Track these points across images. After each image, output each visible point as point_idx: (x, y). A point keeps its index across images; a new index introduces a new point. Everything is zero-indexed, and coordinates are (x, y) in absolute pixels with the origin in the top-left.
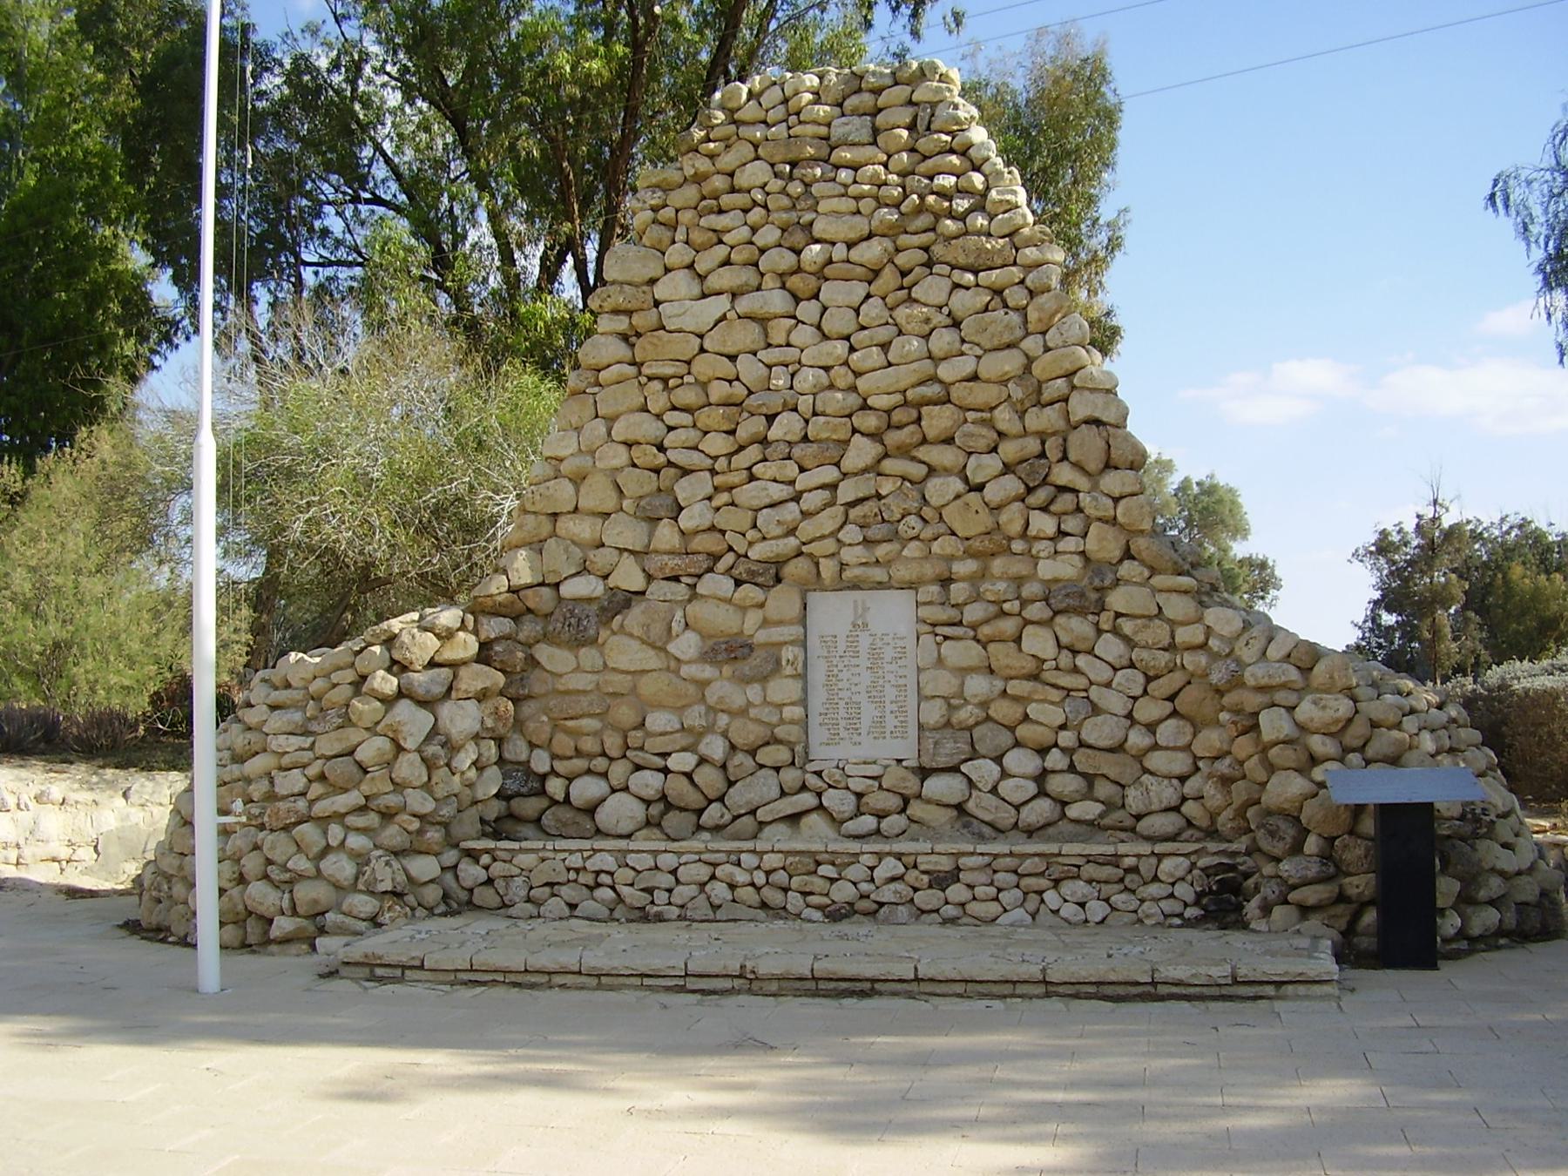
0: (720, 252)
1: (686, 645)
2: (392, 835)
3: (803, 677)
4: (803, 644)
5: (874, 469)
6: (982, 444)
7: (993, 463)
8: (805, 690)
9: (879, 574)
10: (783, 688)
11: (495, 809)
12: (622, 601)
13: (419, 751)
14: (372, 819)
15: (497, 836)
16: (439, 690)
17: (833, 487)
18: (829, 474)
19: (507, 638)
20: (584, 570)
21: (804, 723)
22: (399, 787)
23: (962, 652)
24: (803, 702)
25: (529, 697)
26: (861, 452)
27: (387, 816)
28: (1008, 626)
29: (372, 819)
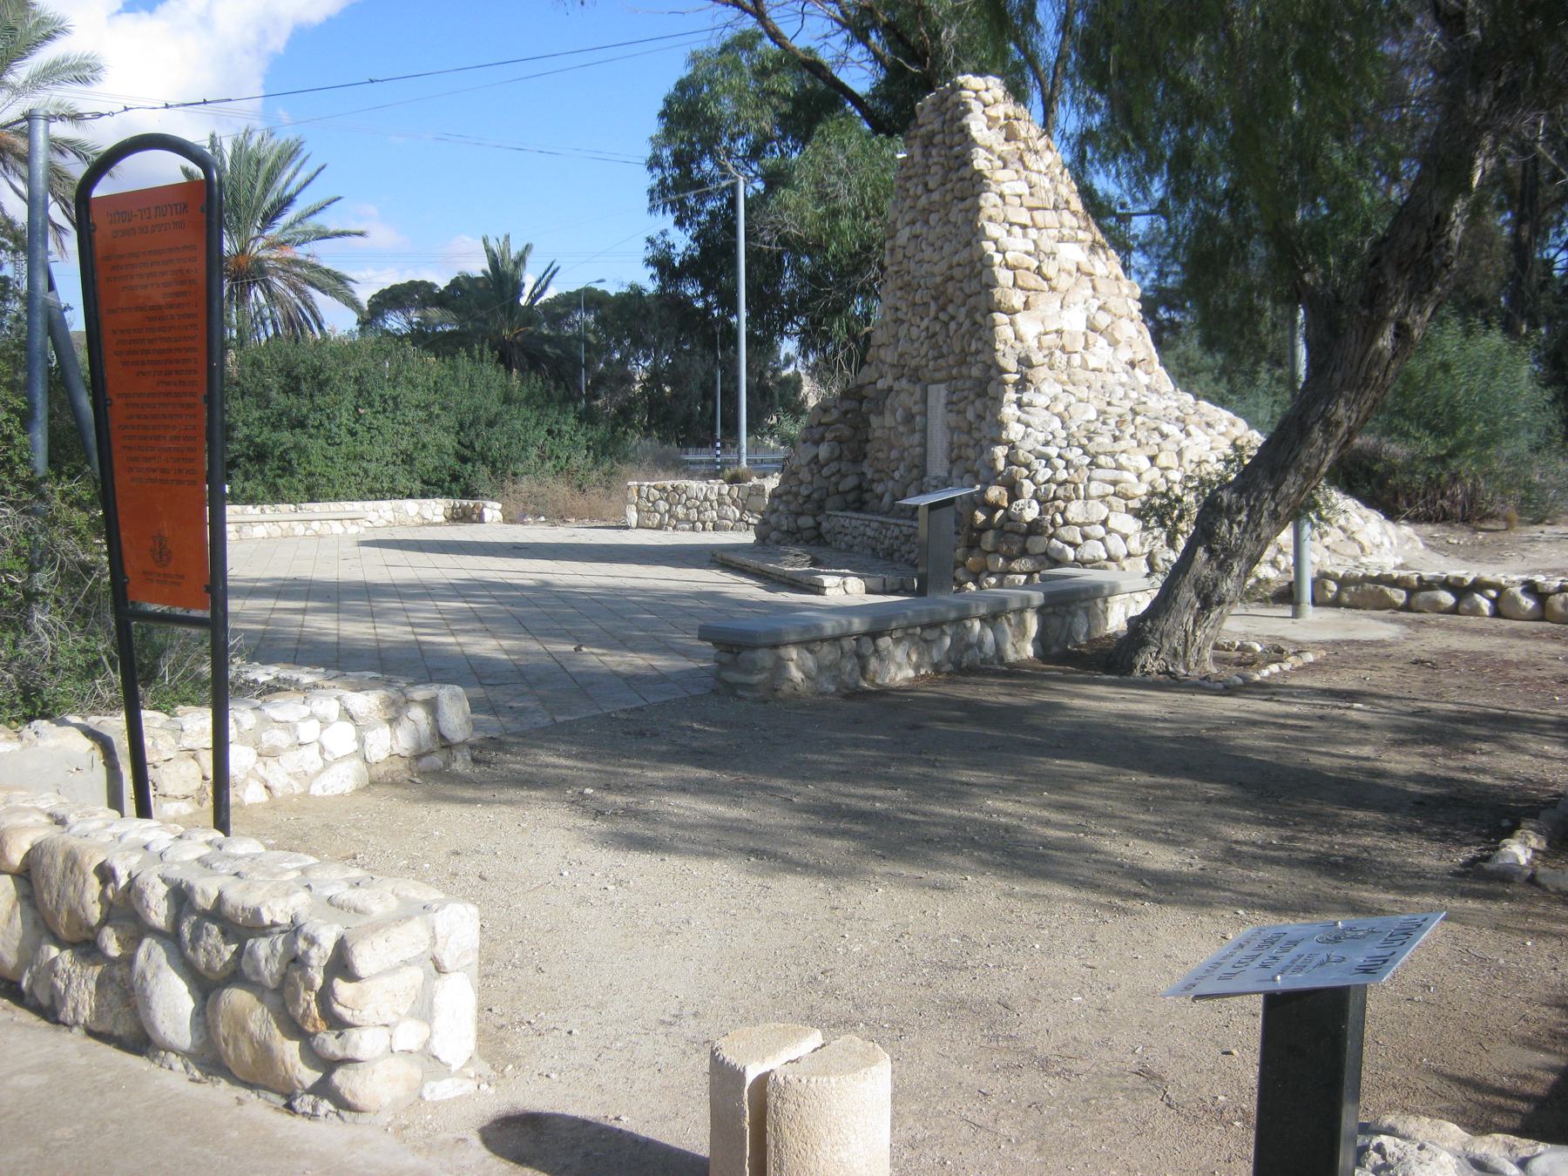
0: (908, 203)
1: (899, 414)
2: (792, 507)
3: (924, 430)
4: (924, 414)
5: (936, 318)
6: (958, 301)
7: (963, 310)
8: (925, 437)
9: (938, 376)
10: (917, 437)
11: (850, 497)
12: (890, 389)
13: (809, 464)
14: (790, 497)
15: (858, 510)
16: (817, 436)
17: (927, 328)
18: (926, 322)
19: (853, 411)
20: (881, 377)
21: (924, 456)
22: (801, 483)
23: (952, 418)
24: (924, 444)
25: (868, 440)
26: (933, 307)
27: (797, 495)
28: (962, 405)
29: (790, 497)
